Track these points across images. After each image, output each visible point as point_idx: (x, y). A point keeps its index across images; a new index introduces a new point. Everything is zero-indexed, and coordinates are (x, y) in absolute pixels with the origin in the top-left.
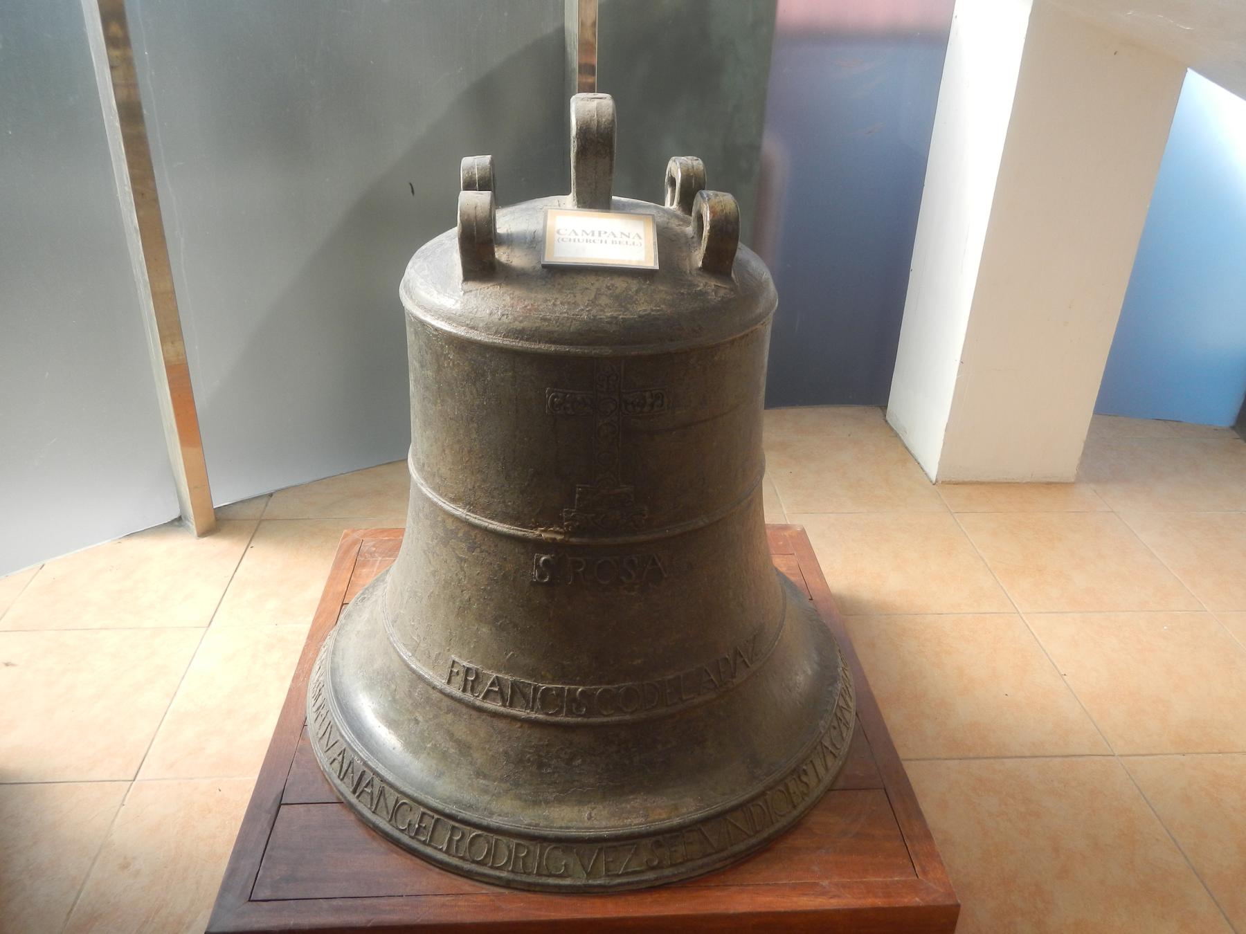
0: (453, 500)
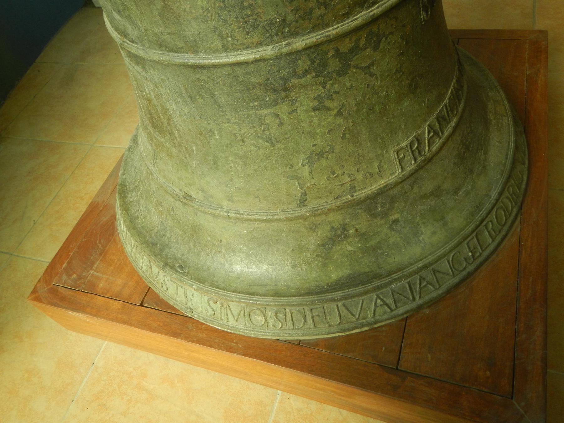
0: (346, 15)
